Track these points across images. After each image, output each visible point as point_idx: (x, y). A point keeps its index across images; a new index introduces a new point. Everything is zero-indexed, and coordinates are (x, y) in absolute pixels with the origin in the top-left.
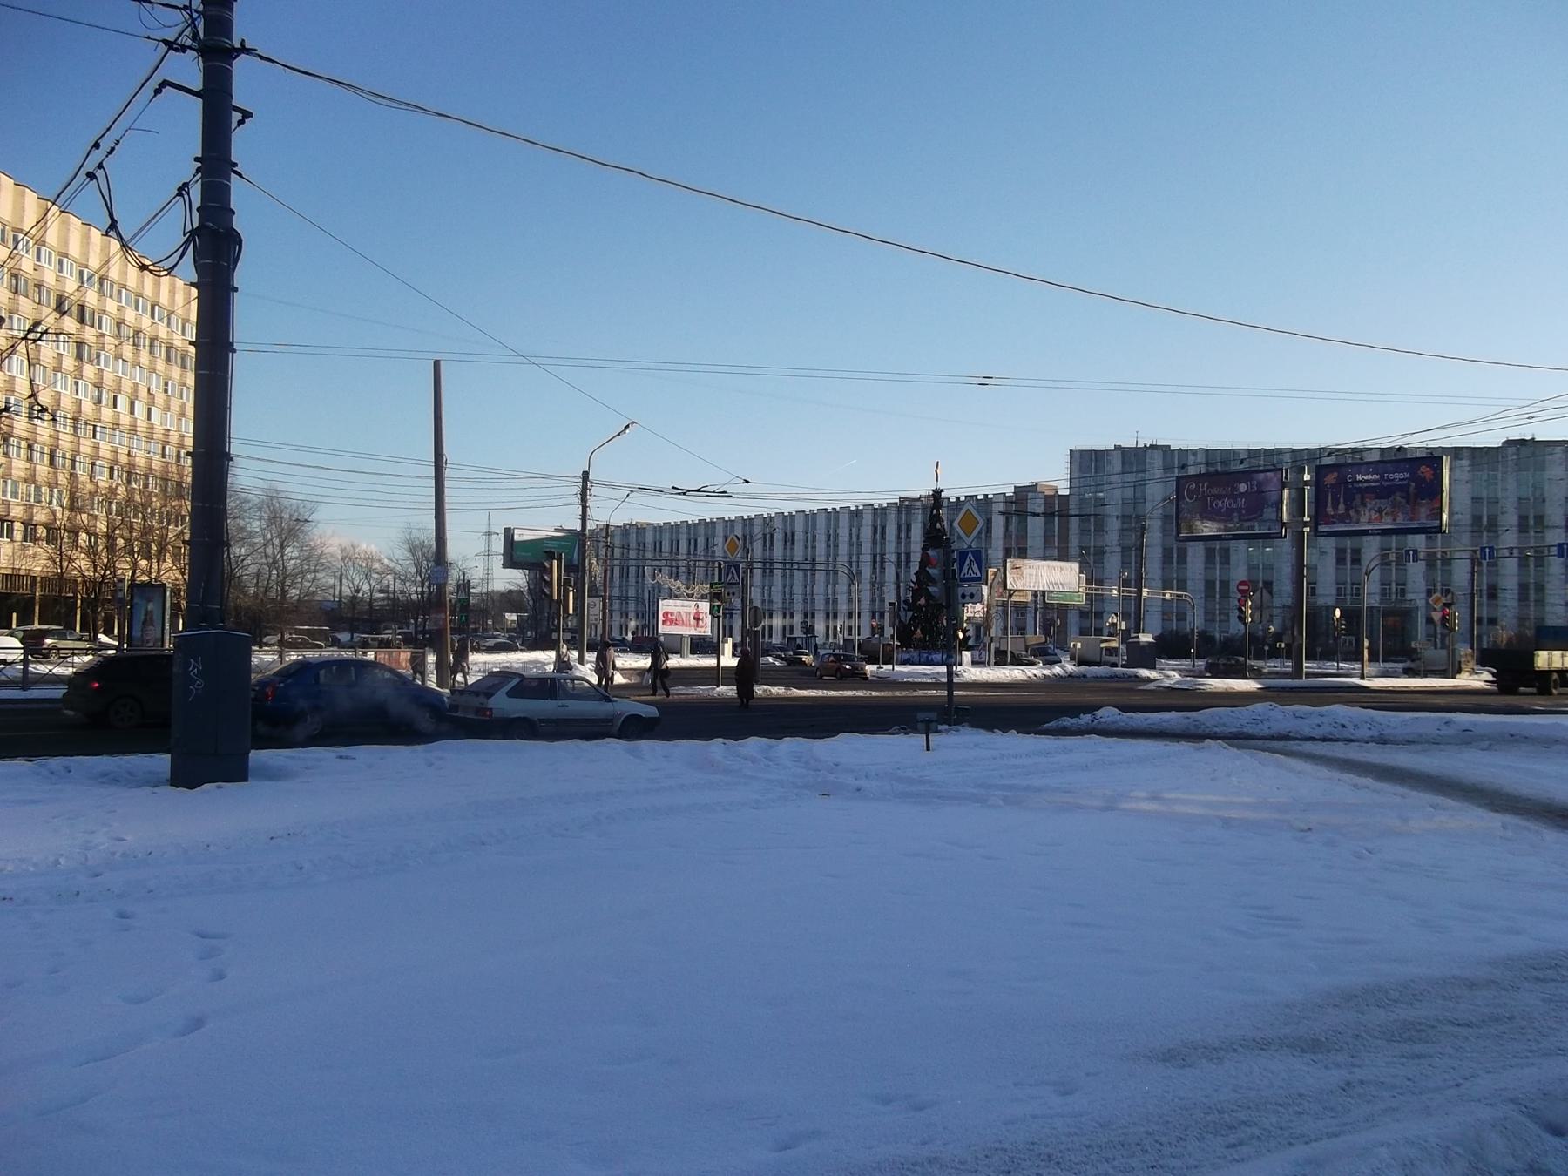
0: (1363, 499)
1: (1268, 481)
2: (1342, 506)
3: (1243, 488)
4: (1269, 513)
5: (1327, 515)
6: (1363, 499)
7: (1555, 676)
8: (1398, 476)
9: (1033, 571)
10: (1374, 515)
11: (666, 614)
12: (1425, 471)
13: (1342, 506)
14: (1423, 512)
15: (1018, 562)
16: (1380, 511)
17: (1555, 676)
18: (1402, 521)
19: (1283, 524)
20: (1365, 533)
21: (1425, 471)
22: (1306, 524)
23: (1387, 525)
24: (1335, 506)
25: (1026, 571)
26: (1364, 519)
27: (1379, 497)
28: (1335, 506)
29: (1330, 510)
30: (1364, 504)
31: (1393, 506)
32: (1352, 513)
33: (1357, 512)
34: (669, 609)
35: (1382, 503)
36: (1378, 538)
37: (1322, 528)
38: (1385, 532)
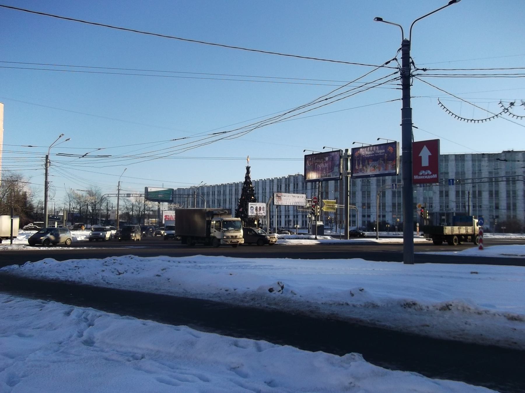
0: (368, 162)
1: (335, 155)
2: (361, 165)
3: (327, 159)
4: (336, 169)
5: (356, 170)
6: (368, 162)
7: (455, 237)
8: (381, 151)
9: (285, 198)
10: (372, 168)
11: (166, 216)
12: (390, 149)
13: (361, 165)
14: (390, 166)
15: (279, 194)
16: (374, 167)
17: (455, 237)
18: (382, 171)
19: (341, 174)
20: (369, 176)
21: (390, 149)
22: (348, 173)
23: (377, 172)
24: (359, 166)
25: (283, 198)
26: (368, 171)
27: (374, 160)
28: (359, 166)
29: (357, 167)
30: (369, 164)
31: (379, 164)
32: (364, 168)
33: (366, 167)
34: (167, 214)
35: (375, 163)
36: (375, 178)
37: (354, 175)
38: (376, 176)
